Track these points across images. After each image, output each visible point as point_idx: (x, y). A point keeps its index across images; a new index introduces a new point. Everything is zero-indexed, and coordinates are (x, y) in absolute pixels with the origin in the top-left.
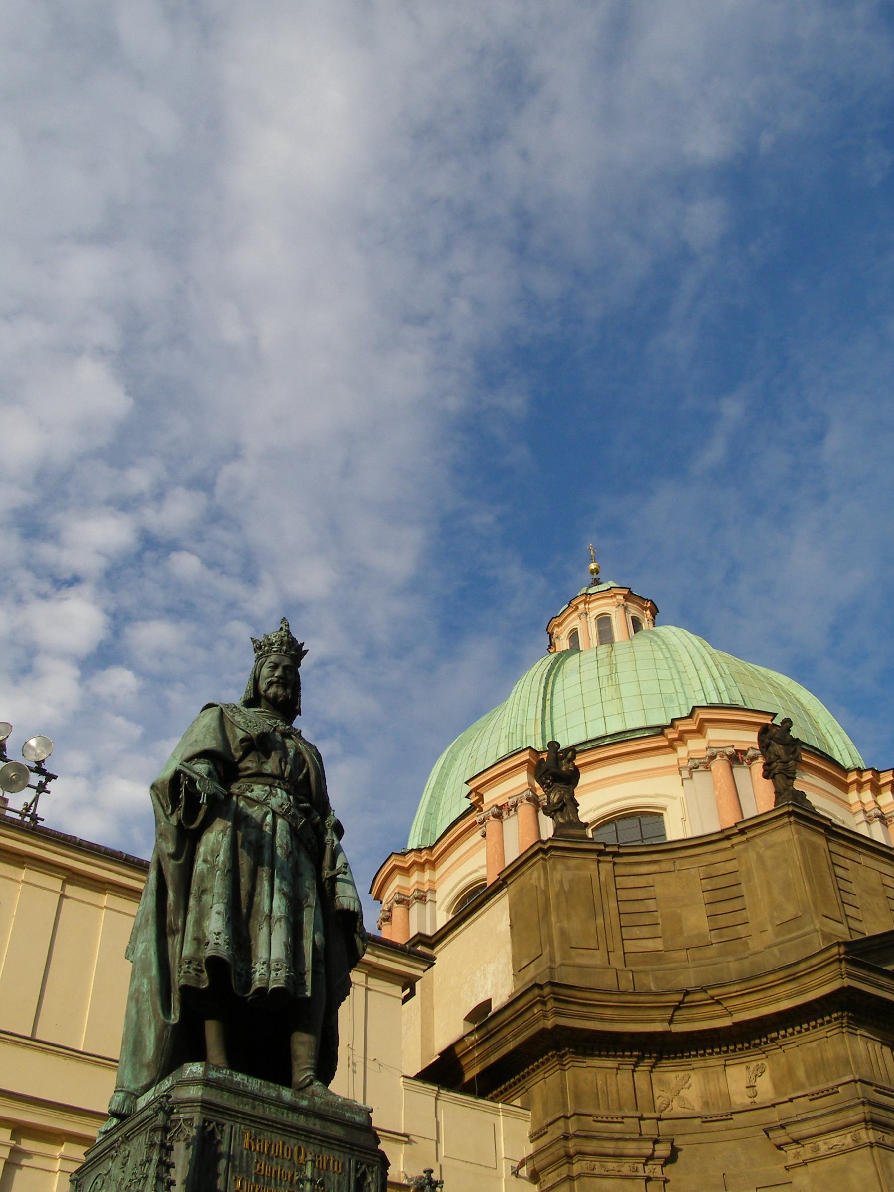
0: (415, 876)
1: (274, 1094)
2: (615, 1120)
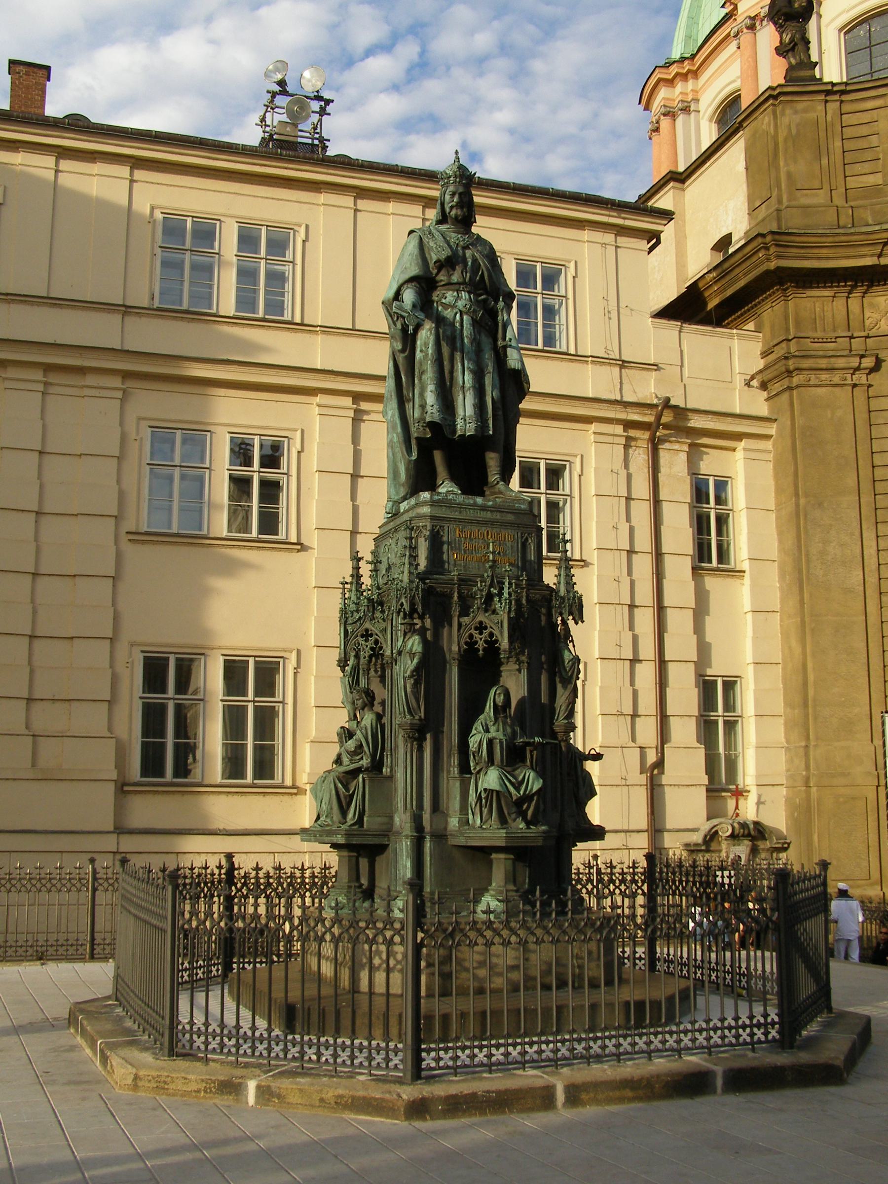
0: (679, 87)
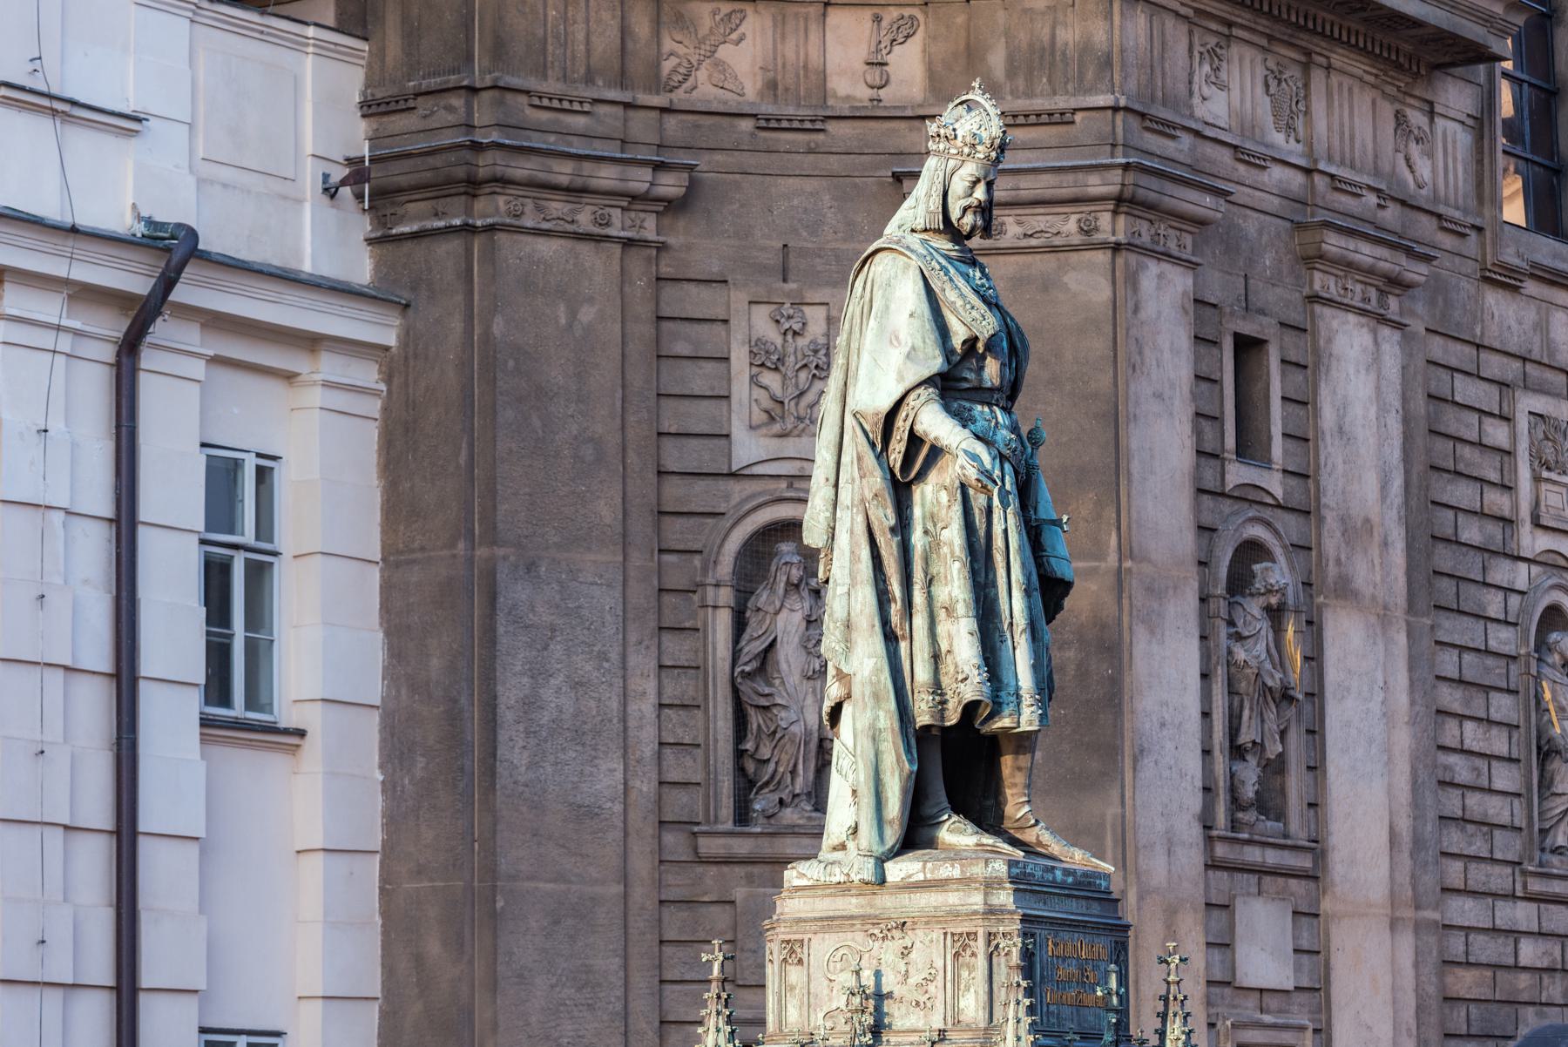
2: (577, 107)
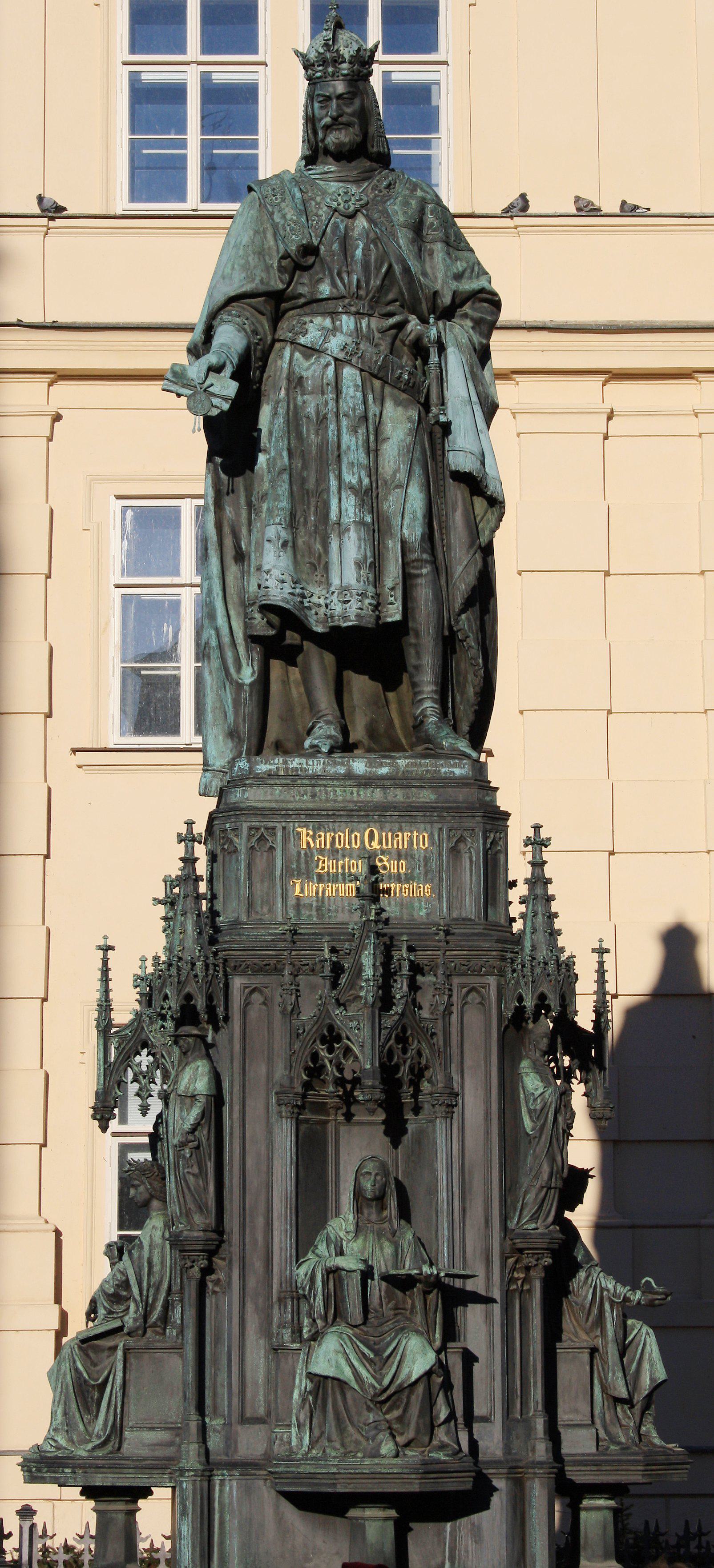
1: (342, 770)
